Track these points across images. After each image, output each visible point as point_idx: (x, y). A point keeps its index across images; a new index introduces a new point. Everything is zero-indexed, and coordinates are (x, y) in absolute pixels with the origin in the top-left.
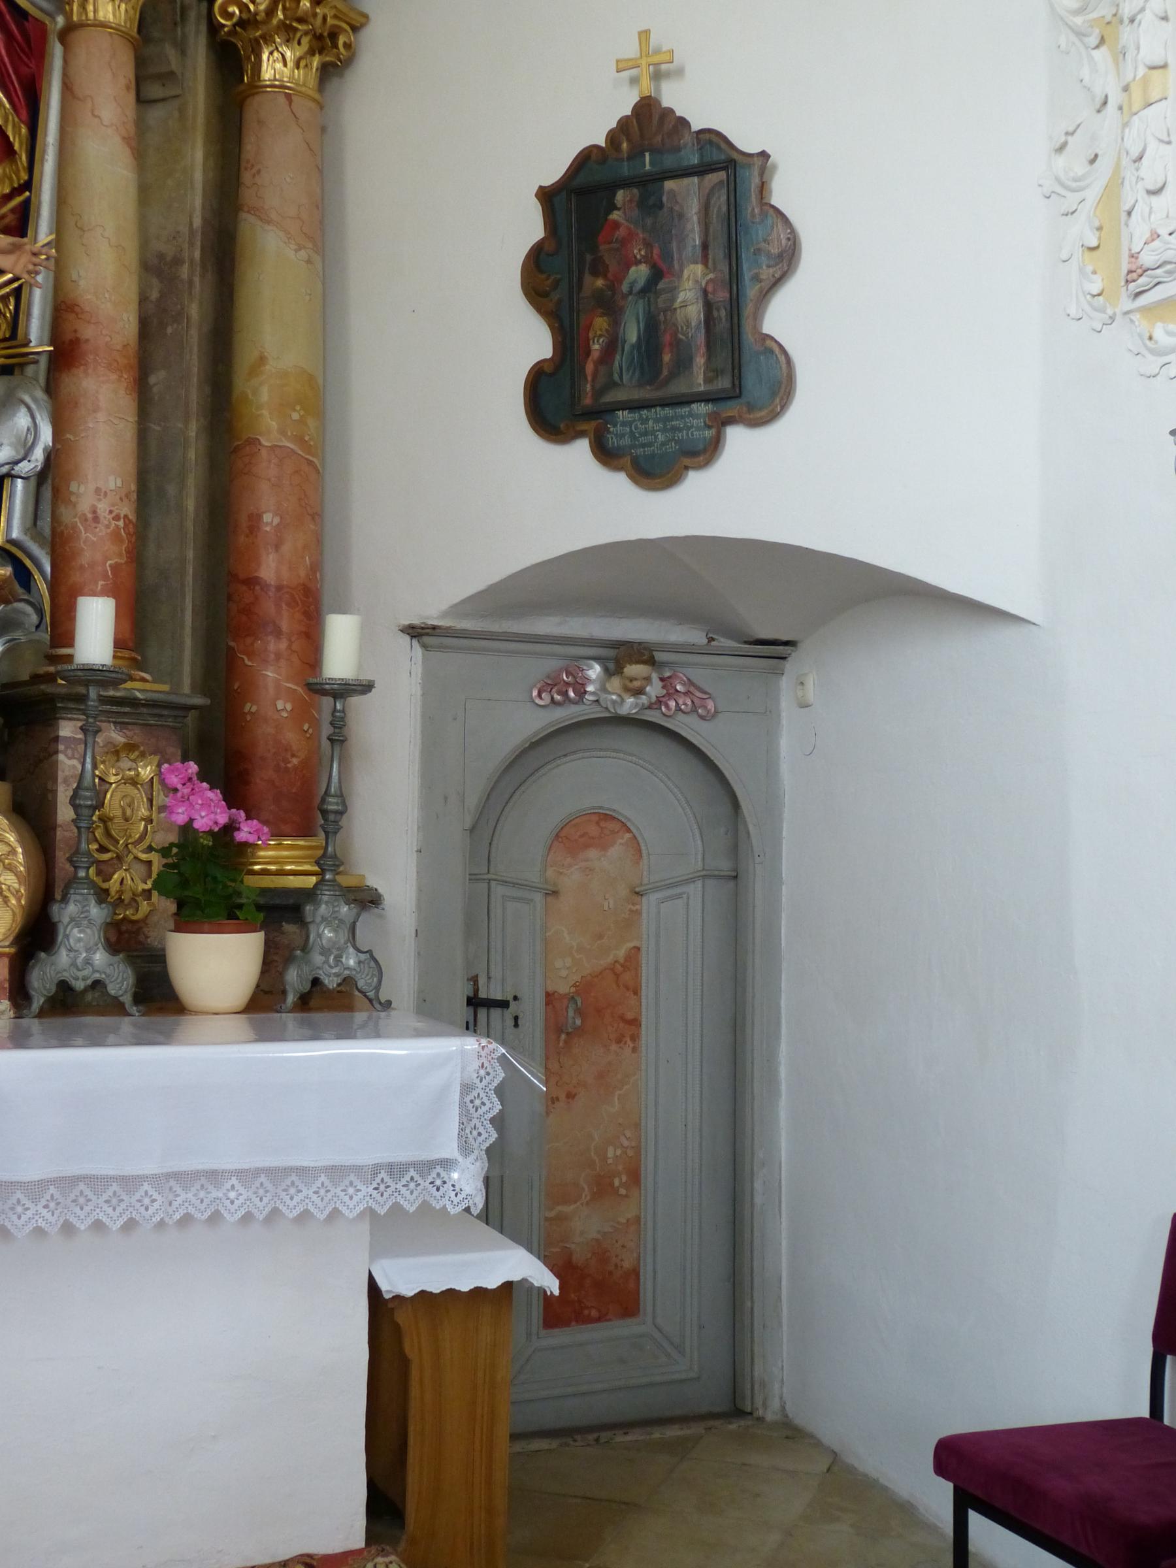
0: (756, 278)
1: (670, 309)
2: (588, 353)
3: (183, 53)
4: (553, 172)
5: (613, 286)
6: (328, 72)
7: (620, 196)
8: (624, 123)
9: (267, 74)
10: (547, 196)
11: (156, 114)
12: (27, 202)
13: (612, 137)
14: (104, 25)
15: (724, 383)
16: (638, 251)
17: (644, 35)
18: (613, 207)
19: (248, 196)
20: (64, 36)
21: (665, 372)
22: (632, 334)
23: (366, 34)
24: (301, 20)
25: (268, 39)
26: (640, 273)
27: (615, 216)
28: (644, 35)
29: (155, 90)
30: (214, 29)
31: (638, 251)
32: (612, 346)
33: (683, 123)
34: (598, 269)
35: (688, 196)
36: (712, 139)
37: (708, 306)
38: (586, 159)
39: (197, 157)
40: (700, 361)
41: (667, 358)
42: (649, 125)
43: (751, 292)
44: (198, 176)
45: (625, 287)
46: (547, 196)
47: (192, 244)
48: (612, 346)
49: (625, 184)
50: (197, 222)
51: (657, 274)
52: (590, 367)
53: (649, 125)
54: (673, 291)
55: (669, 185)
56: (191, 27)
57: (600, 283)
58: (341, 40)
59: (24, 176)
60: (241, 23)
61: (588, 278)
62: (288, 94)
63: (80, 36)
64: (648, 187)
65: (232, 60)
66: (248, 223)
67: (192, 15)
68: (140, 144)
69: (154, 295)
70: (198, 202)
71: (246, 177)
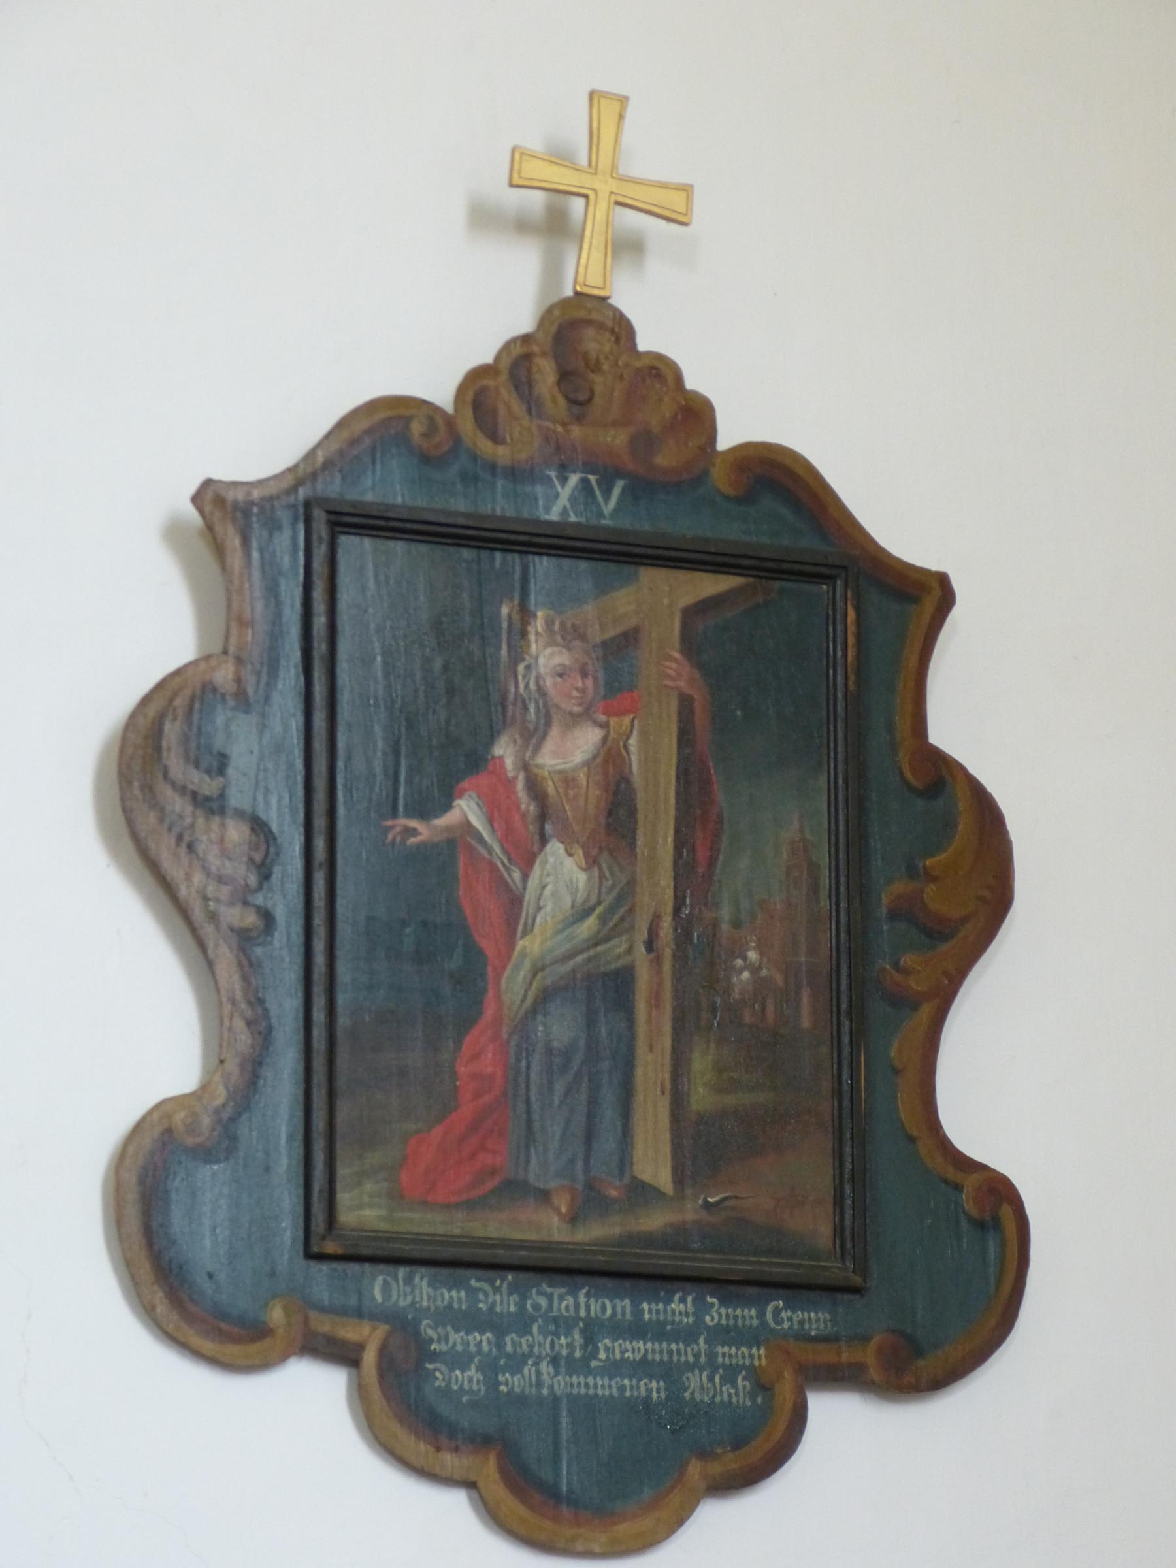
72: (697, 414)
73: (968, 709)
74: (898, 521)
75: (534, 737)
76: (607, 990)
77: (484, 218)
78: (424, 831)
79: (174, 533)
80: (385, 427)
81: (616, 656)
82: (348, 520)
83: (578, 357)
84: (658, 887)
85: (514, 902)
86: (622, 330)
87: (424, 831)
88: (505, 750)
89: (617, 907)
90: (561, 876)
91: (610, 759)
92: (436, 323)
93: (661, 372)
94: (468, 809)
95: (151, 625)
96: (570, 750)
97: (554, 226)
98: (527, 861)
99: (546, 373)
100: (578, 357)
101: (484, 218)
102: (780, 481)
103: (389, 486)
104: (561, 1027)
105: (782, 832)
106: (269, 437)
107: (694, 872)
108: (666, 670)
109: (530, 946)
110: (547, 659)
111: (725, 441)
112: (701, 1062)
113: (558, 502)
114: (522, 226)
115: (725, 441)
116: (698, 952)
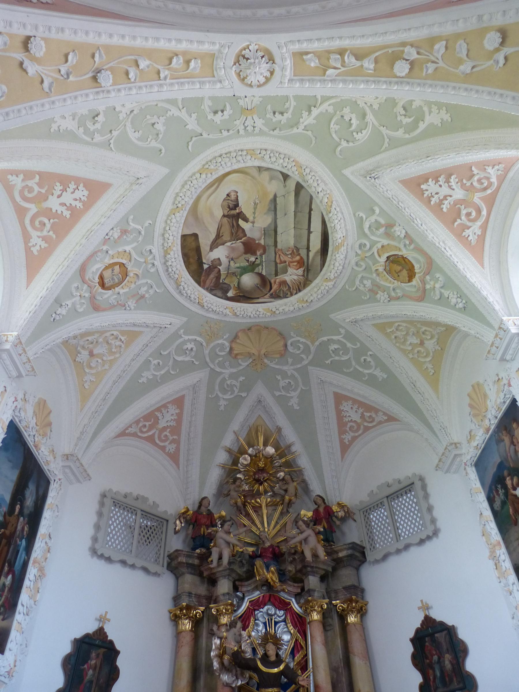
0: (460, 657)
1: (444, 666)
2: (430, 679)
3: (332, 619)
4: (412, 635)
5: (431, 662)
6: (362, 617)
7: (427, 639)
8: (423, 621)
9: (349, 621)
10: (412, 640)
11: (329, 633)
12: (307, 659)
13: (421, 625)
14: (316, 620)
15: (461, 685)
16: (434, 652)
17: (422, 601)
18: (426, 642)
19: (350, 649)
20: (309, 623)
21: (448, 683)
22: (438, 674)
23: (368, 605)
24: (354, 608)
25: (348, 613)
26: (435, 658)
27: (427, 644)
28: (422, 601)
29: (328, 628)
30: (338, 612)
31: (434, 652)
32: (435, 677)
33: (435, 620)
34: (427, 658)
35: (441, 637)
36: (442, 624)
37: (452, 664)
38: (418, 631)
39: (339, 642)
40: (455, 679)
41: (447, 679)
42: (428, 621)
43: (461, 660)
44: (340, 647)
45: (433, 661)
46: (412, 640)
47: (341, 663)
48: (435, 677)
49: (427, 636)
50: (341, 657)
51: (439, 658)
52: (431, 683)
53: (428, 621)
54: (444, 661)
55: (436, 635)
56: (333, 613)
57: (428, 661)
58: (363, 608)
59: (305, 652)
60: (343, 610)
61: (425, 660)
62: (354, 624)
63: (312, 623)
64: (432, 635)
65: (342, 618)
66: (351, 656)
67: (333, 610)
68: (327, 643)
69: (335, 676)
70: (341, 652)
71: (349, 645)
72: (107, 637)
73: (120, 662)
74: (118, 647)
75: (91, 661)
76: (91, 682)
77: (96, 619)
78: (82, 667)
79: (71, 641)
80: (87, 636)
81: (98, 656)
82: (84, 642)
83: (101, 632)
84: (96, 675)
85: (87, 674)
86: (104, 629)
87: (82, 667)
88: (89, 661)
89: (93, 675)
90: (91, 672)
91: (96, 663)
92: (91, 628)
93: (105, 633)
94: (86, 666)
95: (67, 649)
96: (93, 662)
97: (100, 620)
98: (89, 671)
99: (98, 632)
100: (101, 632)
101: (96, 619)
102: (111, 642)
103: (87, 640)
104: (88, 685)
105: (106, 670)
106: (79, 634)
107: (99, 673)
108: (101, 656)
109: (88, 677)
110: (93, 655)
111: (109, 639)
112: (96, 688)
113: (97, 642)
114: (99, 620)
115: (109, 639)
116: (98, 679)
